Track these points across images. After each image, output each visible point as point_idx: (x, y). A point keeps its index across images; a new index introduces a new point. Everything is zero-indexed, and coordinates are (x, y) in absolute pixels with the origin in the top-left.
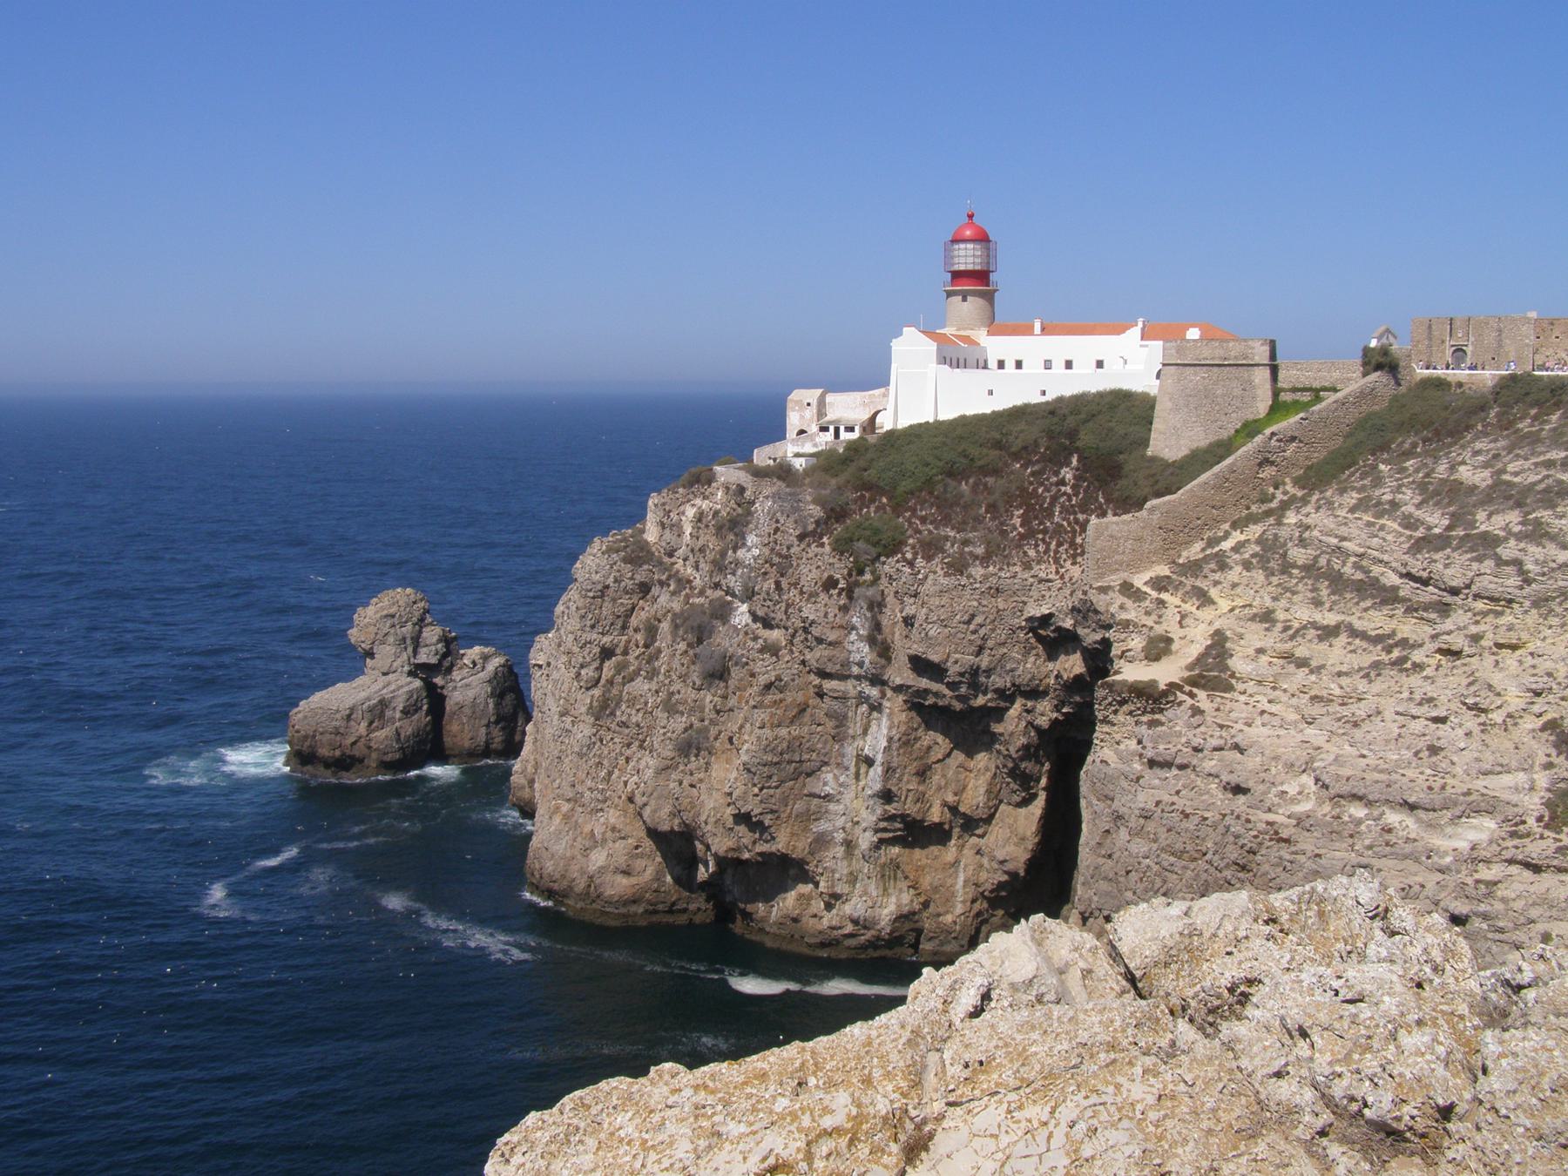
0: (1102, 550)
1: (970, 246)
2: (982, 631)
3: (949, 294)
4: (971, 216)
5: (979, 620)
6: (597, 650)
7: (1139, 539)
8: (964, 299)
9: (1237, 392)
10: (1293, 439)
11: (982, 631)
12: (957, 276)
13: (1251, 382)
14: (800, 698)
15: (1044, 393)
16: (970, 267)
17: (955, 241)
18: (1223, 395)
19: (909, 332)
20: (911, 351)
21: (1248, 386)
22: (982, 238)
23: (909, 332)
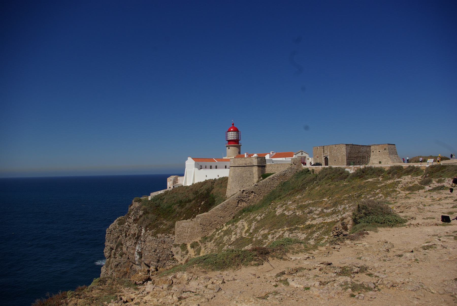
0: (179, 232)
1: (233, 133)
2: (159, 255)
3: (227, 146)
4: (233, 124)
5: (158, 251)
6: (109, 248)
7: (193, 228)
8: (229, 148)
9: (249, 175)
10: (252, 192)
11: (159, 255)
12: (229, 141)
13: (252, 172)
14: (125, 270)
15: (218, 176)
16: (233, 139)
17: (229, 131)
18: (245, 177)
19: (190, 159)
20: (190, 163)
21: (251, 173)
22: (236, 130)
23: (190, 159)
